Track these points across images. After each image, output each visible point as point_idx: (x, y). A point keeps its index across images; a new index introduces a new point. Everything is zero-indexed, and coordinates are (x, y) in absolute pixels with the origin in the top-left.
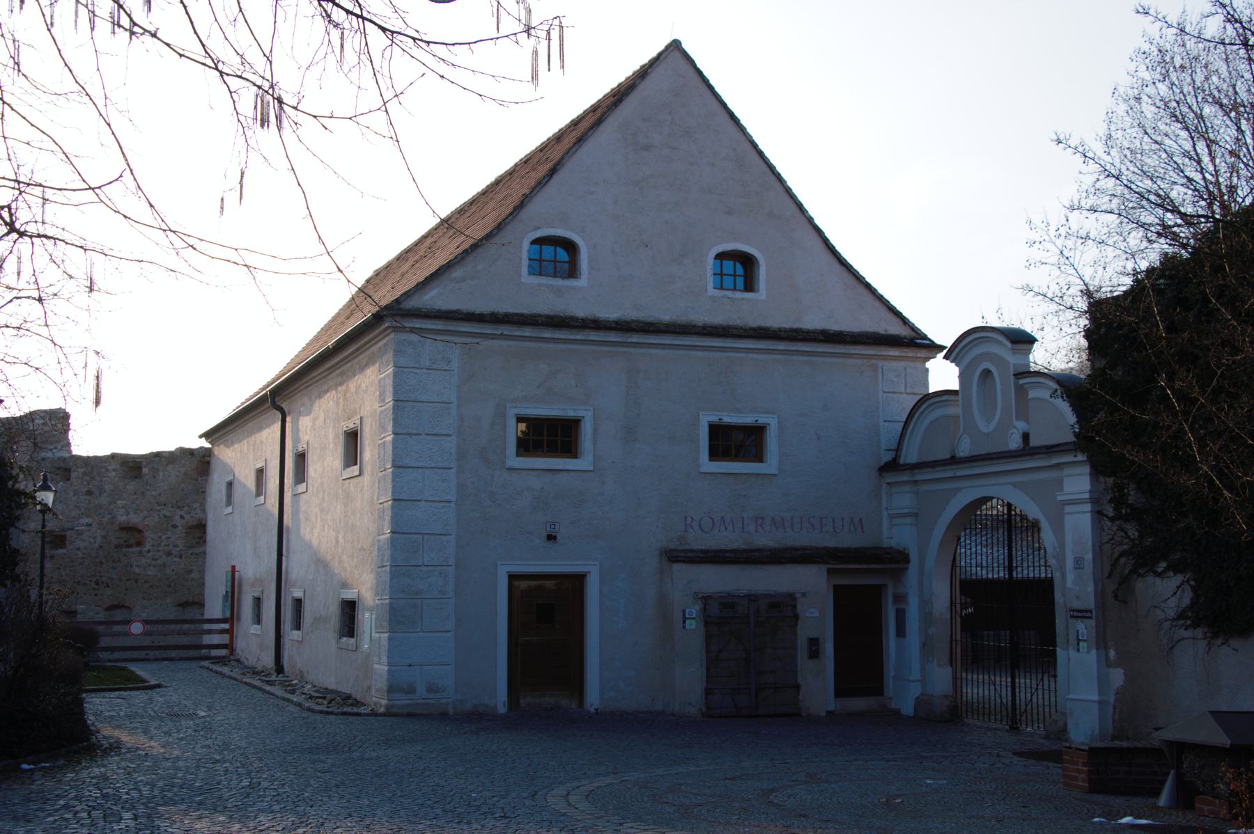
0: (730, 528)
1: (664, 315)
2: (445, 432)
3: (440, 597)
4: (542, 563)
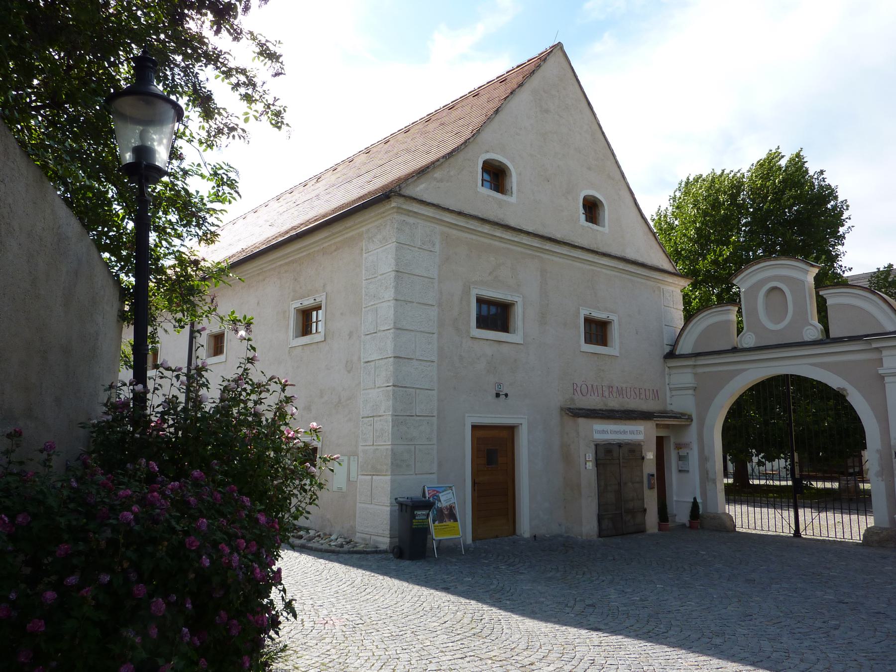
0: (596, 394)
1: (558, 236)
2: (430, 303)
3: (427, 443)
4: (478, 415)
